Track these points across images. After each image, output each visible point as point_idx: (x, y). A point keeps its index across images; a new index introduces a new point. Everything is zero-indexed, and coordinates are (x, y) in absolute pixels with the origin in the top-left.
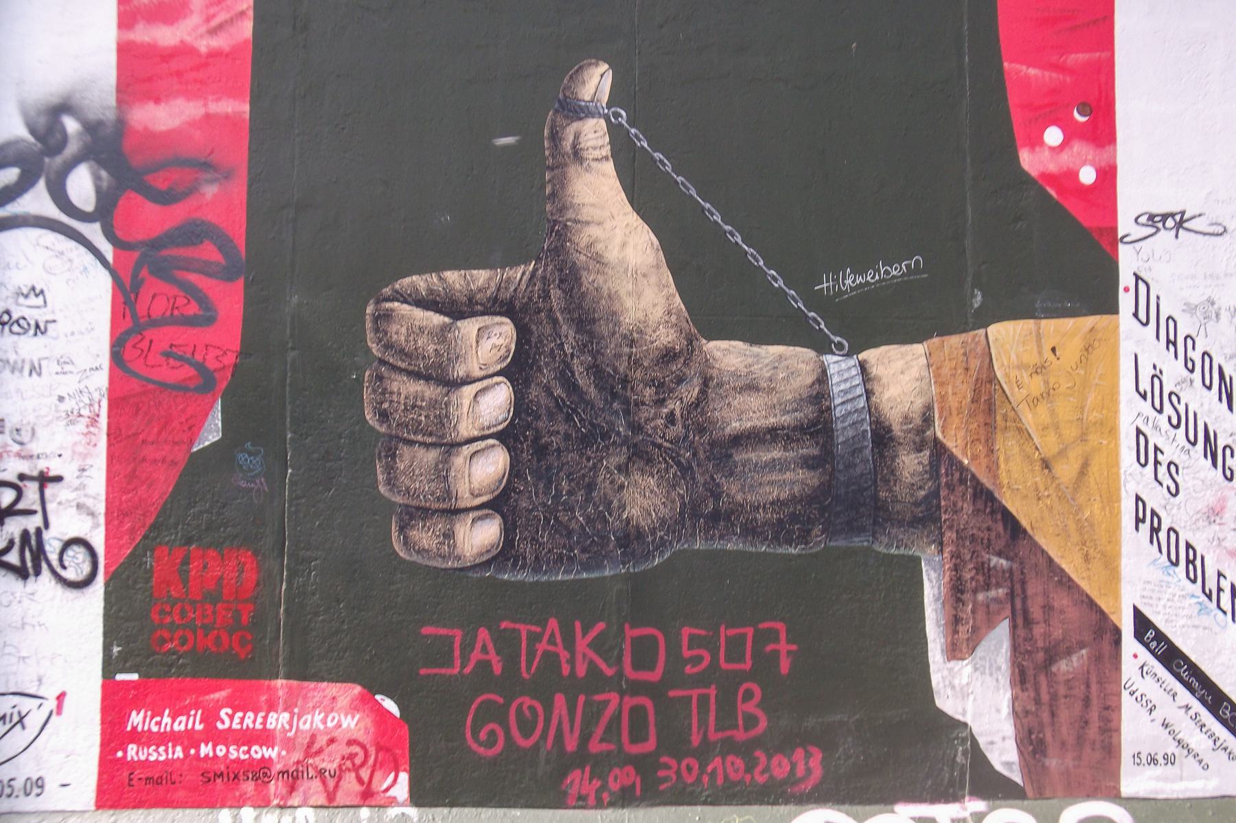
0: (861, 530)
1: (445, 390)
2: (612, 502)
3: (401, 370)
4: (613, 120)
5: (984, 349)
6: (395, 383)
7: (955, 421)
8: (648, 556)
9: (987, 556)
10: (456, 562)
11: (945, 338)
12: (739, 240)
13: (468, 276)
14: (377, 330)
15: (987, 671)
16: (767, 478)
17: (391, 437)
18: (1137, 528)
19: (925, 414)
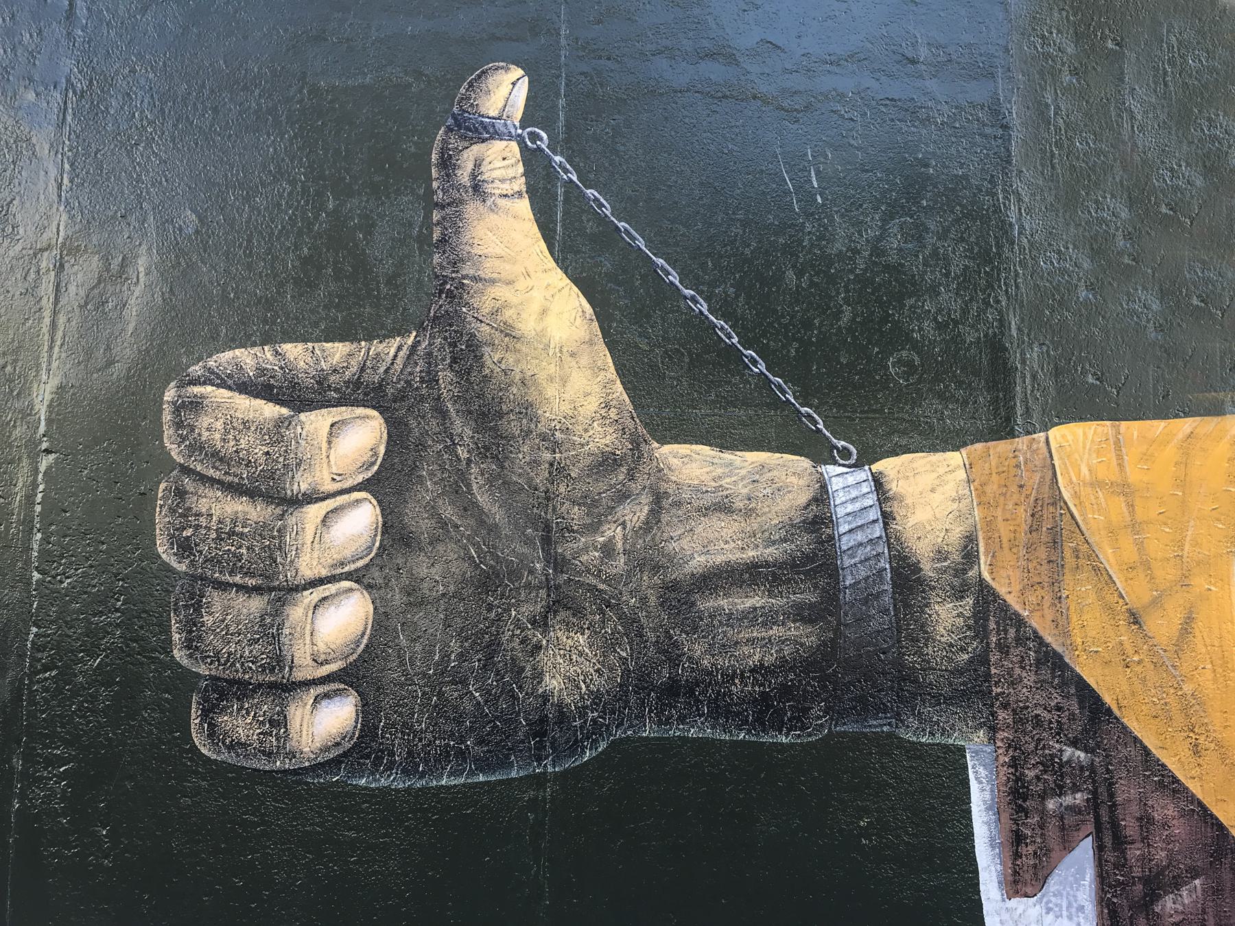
0: (883, 709)
1: (278, 511)
2: (523, 669)
3: (212, 481)
4: (529, 143)
5: (1044, 459)
6: (204, 500)
7: (1006, 556)
8: (575, 747)
9: (1057, 746)
10: (287, 761)
11: (990, 444)
12: (705, 310)
13: (317, 351)
14: (179, 425)
15: (1065, 913)
16: (745, 635)
17: (194, 578)
19: (966, 547)
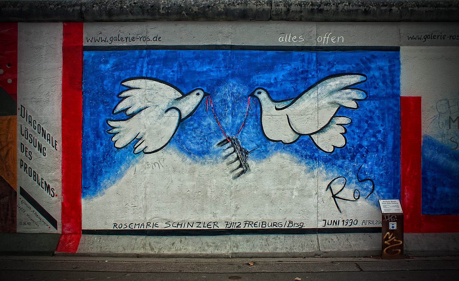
18: (21, 168)
